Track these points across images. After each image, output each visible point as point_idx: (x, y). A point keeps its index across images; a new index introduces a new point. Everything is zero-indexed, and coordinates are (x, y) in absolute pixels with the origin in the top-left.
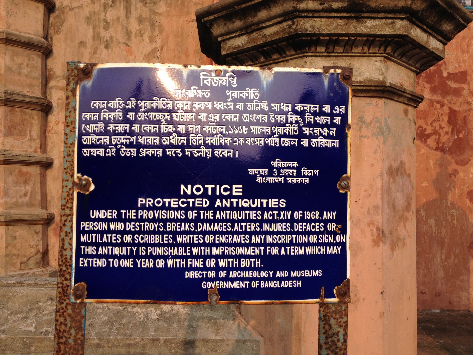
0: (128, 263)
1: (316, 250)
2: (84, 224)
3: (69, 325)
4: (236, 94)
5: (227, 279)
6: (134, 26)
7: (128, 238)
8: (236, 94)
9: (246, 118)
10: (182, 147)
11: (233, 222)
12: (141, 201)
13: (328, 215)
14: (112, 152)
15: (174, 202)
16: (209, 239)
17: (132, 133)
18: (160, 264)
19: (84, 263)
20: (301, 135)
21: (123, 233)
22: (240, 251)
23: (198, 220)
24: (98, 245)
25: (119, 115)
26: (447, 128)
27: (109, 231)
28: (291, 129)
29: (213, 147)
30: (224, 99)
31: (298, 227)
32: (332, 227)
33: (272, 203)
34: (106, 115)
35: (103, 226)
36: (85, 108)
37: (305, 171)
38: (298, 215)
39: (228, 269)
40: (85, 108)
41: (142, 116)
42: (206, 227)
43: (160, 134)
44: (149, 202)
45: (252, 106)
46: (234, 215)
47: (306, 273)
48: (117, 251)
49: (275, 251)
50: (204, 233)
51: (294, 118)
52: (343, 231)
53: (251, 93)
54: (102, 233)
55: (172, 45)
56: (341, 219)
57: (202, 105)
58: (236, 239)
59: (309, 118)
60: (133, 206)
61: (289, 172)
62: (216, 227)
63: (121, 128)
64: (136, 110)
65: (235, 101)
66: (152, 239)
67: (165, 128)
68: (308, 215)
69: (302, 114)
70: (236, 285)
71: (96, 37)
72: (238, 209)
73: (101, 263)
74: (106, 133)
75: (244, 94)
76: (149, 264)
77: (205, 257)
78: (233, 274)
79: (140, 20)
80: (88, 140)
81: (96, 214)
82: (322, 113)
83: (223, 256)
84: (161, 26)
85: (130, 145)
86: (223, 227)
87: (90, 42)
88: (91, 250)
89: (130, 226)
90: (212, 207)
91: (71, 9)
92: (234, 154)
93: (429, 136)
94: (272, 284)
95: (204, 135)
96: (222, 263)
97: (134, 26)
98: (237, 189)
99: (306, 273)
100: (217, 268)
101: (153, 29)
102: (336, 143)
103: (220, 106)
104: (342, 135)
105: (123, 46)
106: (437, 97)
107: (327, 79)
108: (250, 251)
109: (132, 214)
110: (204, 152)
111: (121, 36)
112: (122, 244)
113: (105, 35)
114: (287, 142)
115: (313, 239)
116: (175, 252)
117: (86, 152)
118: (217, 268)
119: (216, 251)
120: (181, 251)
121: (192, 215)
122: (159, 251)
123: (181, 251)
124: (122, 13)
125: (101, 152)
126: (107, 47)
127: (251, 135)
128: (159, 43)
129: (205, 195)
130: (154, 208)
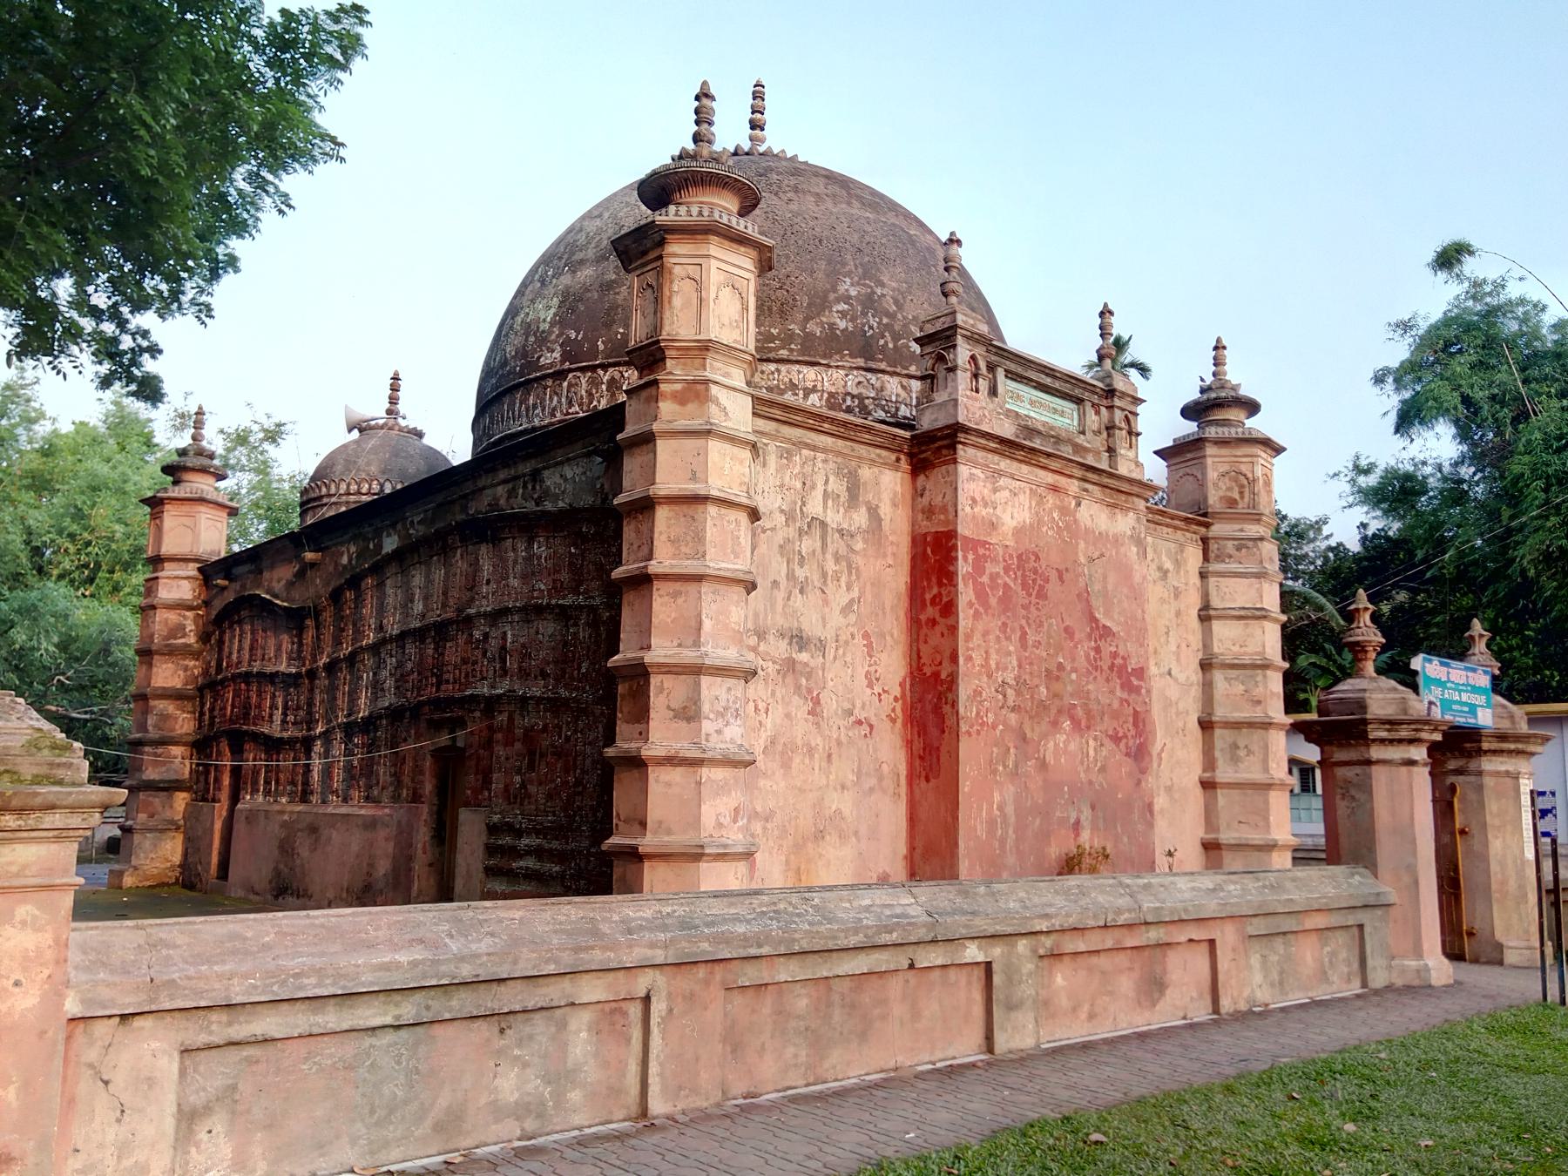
6: (831, 566)
26: (1133, 732)
55: (869, 596)
71: (791, 576)
79: (837, 559)
84: (857, 569)
87: (783, 583)
91: (764, 531)
93: (1120, 739)
97: (831, 566)
101: (850, 573)
105: (818, 592)
106: (1125, 696)
111: (816, 578)
113: (800, 573)
124: (819, 544)
126: (801, 592)
128: (855, 594)
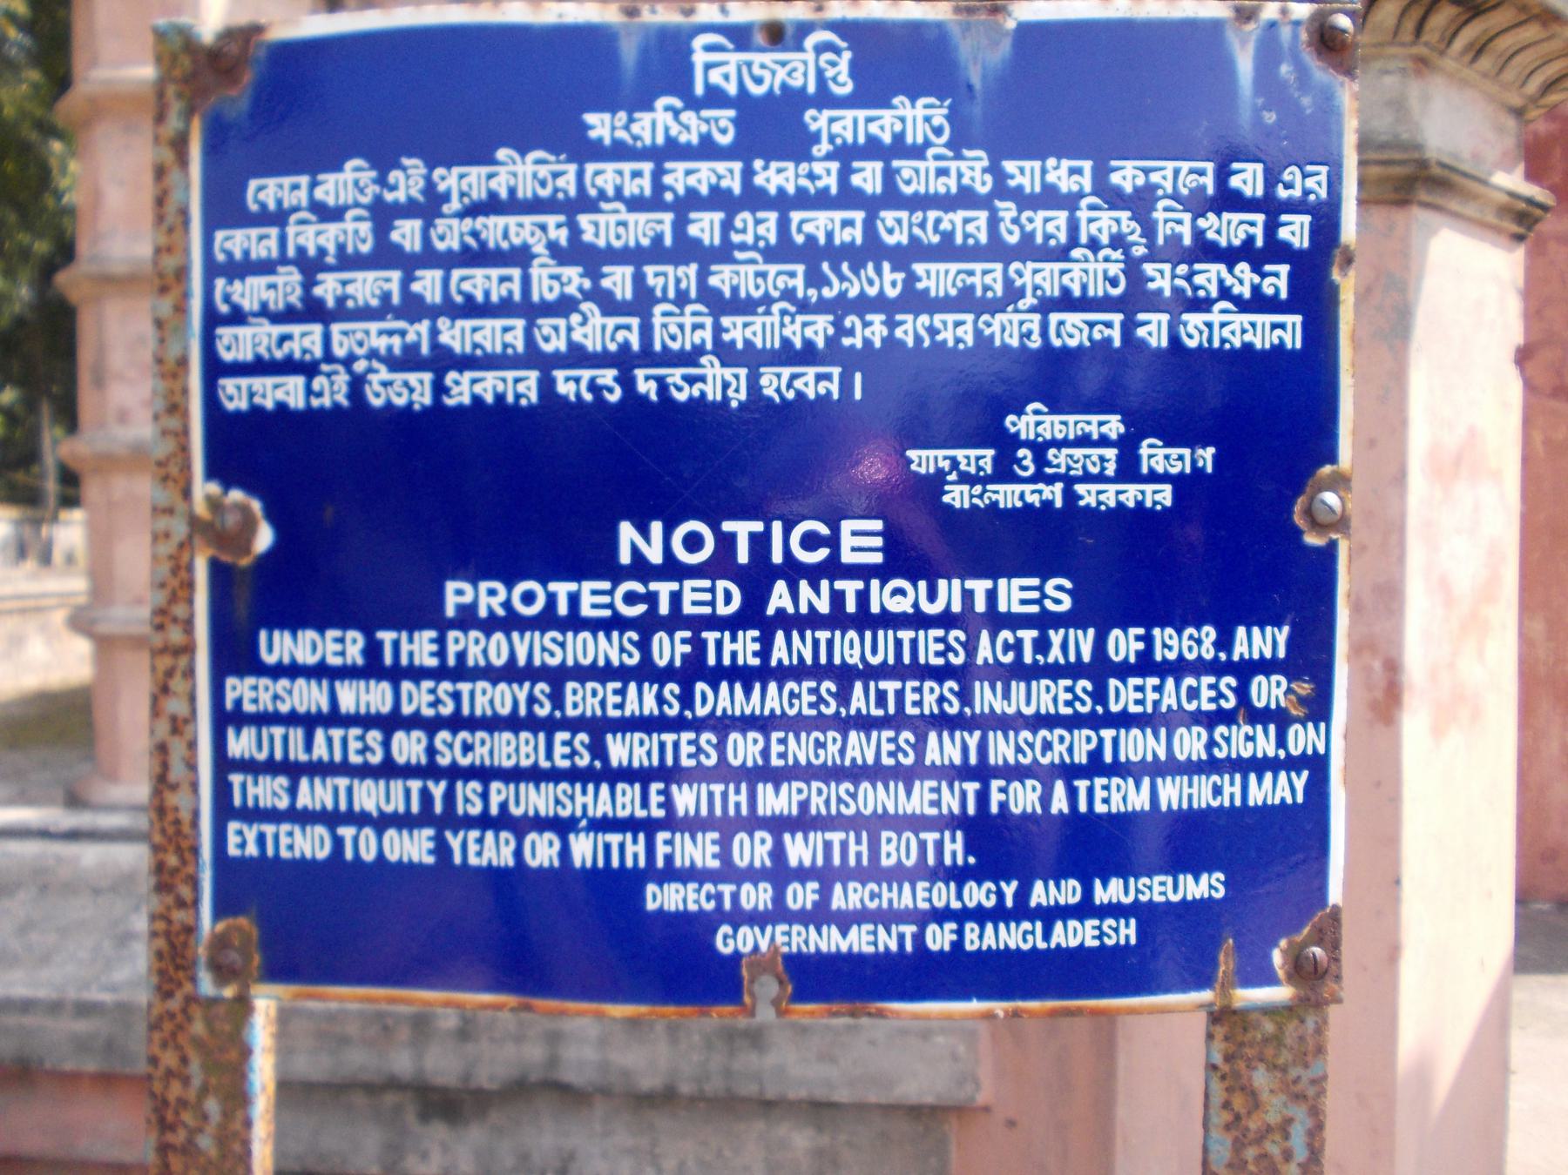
0: (414, 847)
1: (1202, 793)
2: (240, 689)
3: (197, 1082)
4: (848, 124)
5: (819, 915)
7: (409, 747)
8: (848, 124)
9: (895, 227)
10: (624, 361)
11: (845, 676)
12: (456, 594)
13: (1260, 641)
14: (332, 391)
15: (592, 596)
16: (745, 749)
17: (413, 308)
18: (543, 851)
19: (243, 840)
20: (1135, 299)
21: (391, 723)
22: (873, 798)
23: (693, 670)
24: (293, 771)
25: (357, 232)
27: (334, 718)
28: (1092, 273)
29: (752, 358)
30: (798, 146)
31: (1124, 695)
32: (1268, 691)
33: (1014, 594)
34: (310, 236)
35: (309, 696)
36: (226, 208)
37: (1154, 455)
38: (1124, 644)
39: (826, 876)
40: (226, 208)
41: (451, 234)
42: (728, 700)
43: (531, 310)
44: (489, 596)
45: (915, 176)
46: (849, 648)
47: (1158, 889)
48: (369, 795)
49: (1024, 798)
50: (723, 725)
51: (1105, 223)
52: (1318, 709)
53: (916, 116)
54: (310, 722)
56: (1310, 660)
57: (704, 175)
58: (859, 748)
59: (1174, 223)
60: (423, 612)
61: (1085, 460)
62: (773, 699)
63: (366, 286)
64: (429, 206)
65: (846, 155)
66: (507, 749)
67: (546, 281)
68: (1170, 643)
69: (1141, 203)
70: (859, 940)
72: (866, 620)
73: (310, 844)
74: (313, 311)
75: (883, 124)
76: (495, 851)
77: (727, 827)
78: (846, 897)
80: (238, 343)
81: (279, 646)
82: (1228, 200)
83: (803, 822)
85: (407, 360)
86: (801, 698)
88: (268, 791)
89: (417, 698)
90: (751, 615)
92: (846, 385)
94: (1014, 937)
95: (720, 305)
96: (799, 850)
98: (860, 540)
99: (1158, 889)
100: (780, 873)
102: (1290, 331)
103: (776, 177)
104: (1312, 295)
107: (1251, 48)
108: (919, 799)
109: (421, 648)
110: (719, 382)
112: (389, 770)
114: (1073, 330)
115: (1190, 743)
116: (601, 801)
117: (236, 394)
118: (780, 873)
119: (775, 801)
120: (627, 800)
121: (669, 649)
122: (537, 800)
123: (627, 800)
125: (290, 392)
127: (915, 300)
129: (721, 564)
130: (510, 622)
